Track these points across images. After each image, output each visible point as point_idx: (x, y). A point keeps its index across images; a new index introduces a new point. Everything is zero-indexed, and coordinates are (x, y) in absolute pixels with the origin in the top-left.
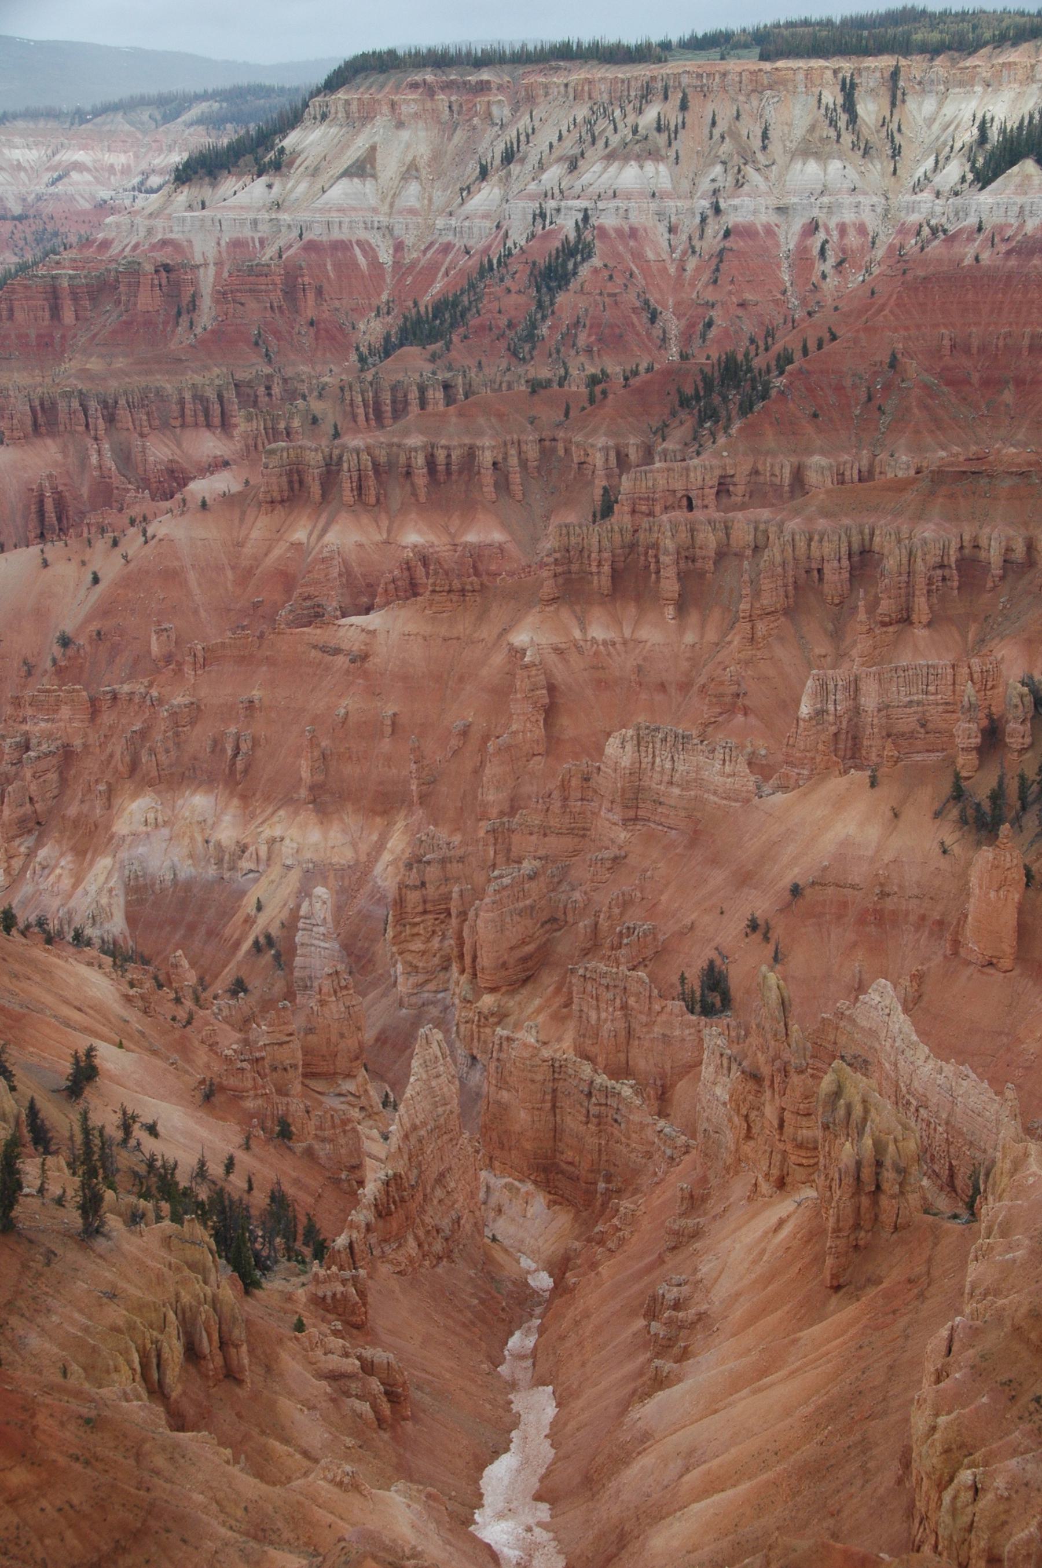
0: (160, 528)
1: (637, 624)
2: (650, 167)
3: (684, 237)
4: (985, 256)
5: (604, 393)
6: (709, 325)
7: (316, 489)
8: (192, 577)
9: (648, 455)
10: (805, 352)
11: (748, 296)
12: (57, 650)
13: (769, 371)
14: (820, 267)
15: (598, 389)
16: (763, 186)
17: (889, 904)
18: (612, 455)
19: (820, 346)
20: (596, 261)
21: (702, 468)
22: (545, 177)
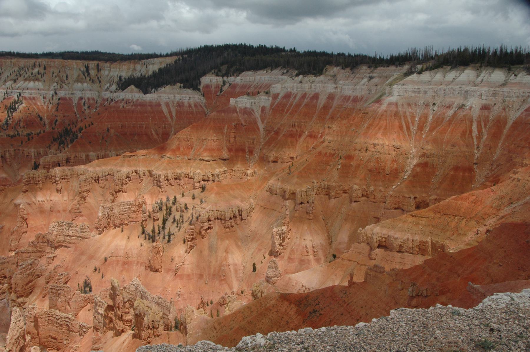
1: (50, 196)
2: (37, 83)
3: (48, 100)
4: (125, 106)
5: (32, 138)
6: (57, 121)
9: (46, 154)
10: (86, 128)
11: (66, 114)
13: (77, 132)
14: (84, 108)
15: (30, 137)
16: (67, 88)
17: (130, 259)
18: (36, 153)
19: (89, 126)
20: (24, 105)
21: (61, 156)
22: (7, 84)
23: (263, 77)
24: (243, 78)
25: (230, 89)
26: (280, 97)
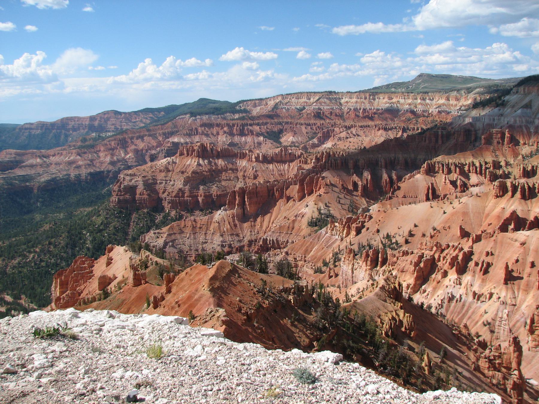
0: (464, 200)
7: (510, 193)
8: (472, 215)
12: (432, 231)
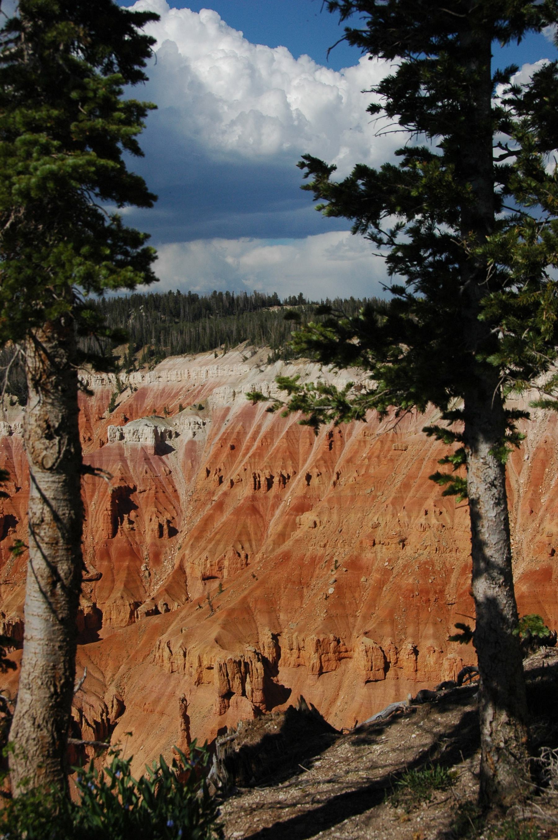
23: (204, 369)
24: (163, 374)
25: (131, 401)
26: (231, 416)
